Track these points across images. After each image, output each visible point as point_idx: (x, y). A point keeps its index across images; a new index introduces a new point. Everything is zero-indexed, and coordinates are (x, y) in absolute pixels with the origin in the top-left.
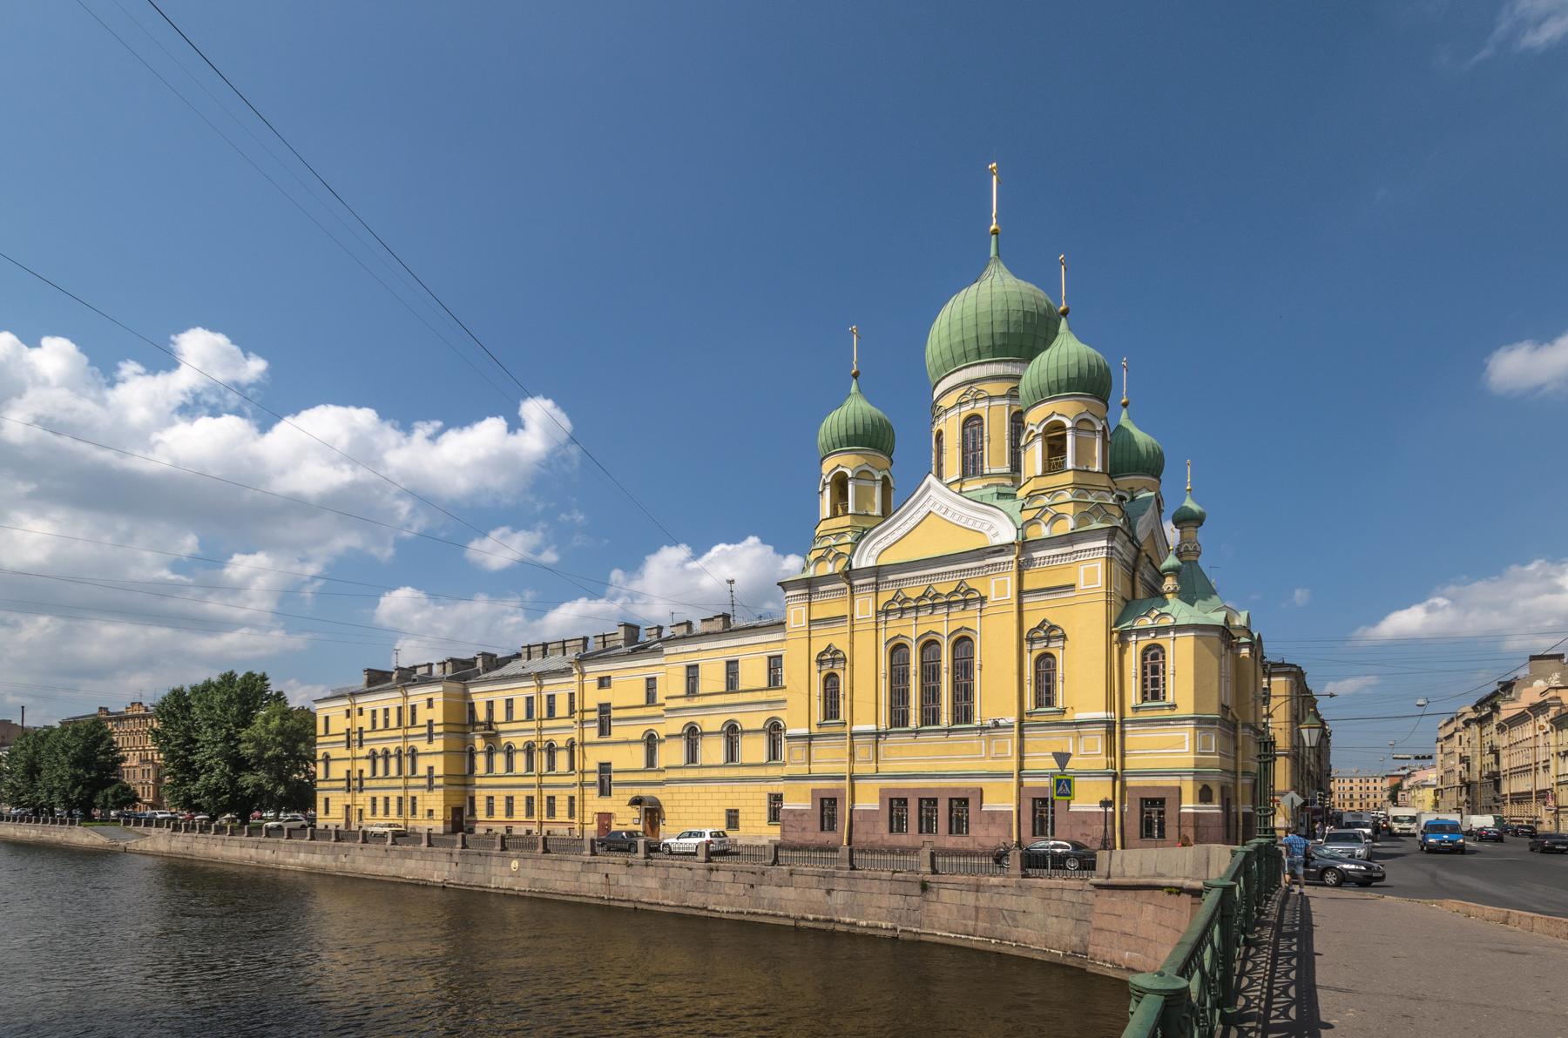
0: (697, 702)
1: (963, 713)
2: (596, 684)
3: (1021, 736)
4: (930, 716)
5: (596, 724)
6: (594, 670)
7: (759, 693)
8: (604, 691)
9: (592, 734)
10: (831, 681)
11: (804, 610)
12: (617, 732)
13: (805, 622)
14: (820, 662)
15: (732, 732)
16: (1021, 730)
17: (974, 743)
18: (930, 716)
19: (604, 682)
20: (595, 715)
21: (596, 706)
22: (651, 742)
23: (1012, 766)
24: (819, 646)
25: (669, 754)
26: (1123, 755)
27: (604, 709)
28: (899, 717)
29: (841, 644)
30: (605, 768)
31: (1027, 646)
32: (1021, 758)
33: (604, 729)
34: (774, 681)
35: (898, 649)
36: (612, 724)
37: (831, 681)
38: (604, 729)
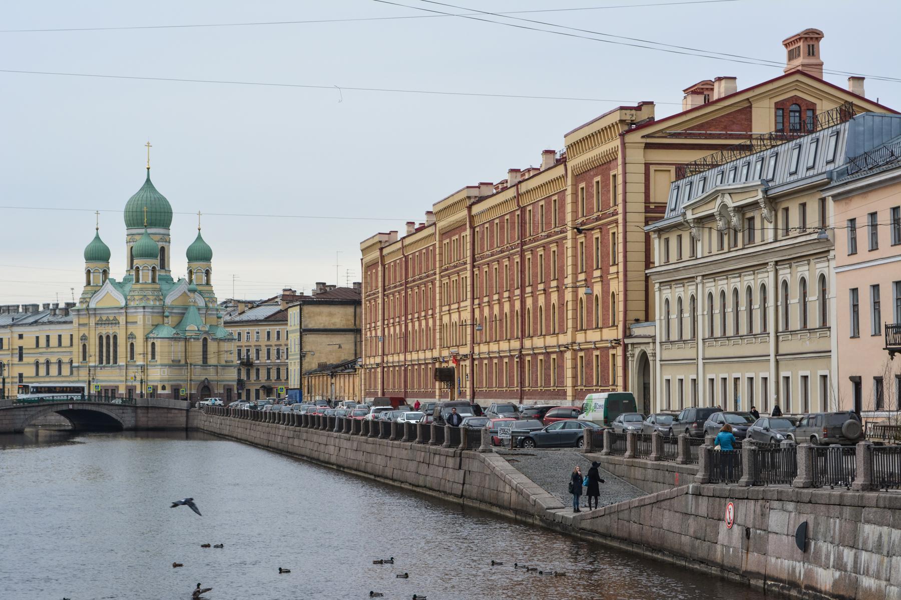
0: (49, 350)
1: (115, 362)
2: (17, 336)
3: (126, 369)
4: (108, 362)
5: (18, 355)
6: (18, 330)
7: (67, 348)
8: (21, 341)
9: (16, 359)
10: (84, 346)
11: (77, 319)
12: (25, 360)
13: (77, 325)
14: (81, 339)
15: (60, 363)
16: (126, 367)
17: (116, 371)
18: (108, 362)
19: (21, 337)
20: (17, 351)
21: (18, 348)
22: (37, 364)
23: (124, 379)
24: (81, 334)
25: (42, 371)
26: (147, 376)
27: (21, 348)
28: (101, 362)
29: (87, 334)
30: (21, 376)
31: (128, 340)
32: (126, 376)
33: (21, 359)
34: (71, 345)
35: (101, 338)
36: (24, 356)
37: (84, 346)
38: (21, 359)
